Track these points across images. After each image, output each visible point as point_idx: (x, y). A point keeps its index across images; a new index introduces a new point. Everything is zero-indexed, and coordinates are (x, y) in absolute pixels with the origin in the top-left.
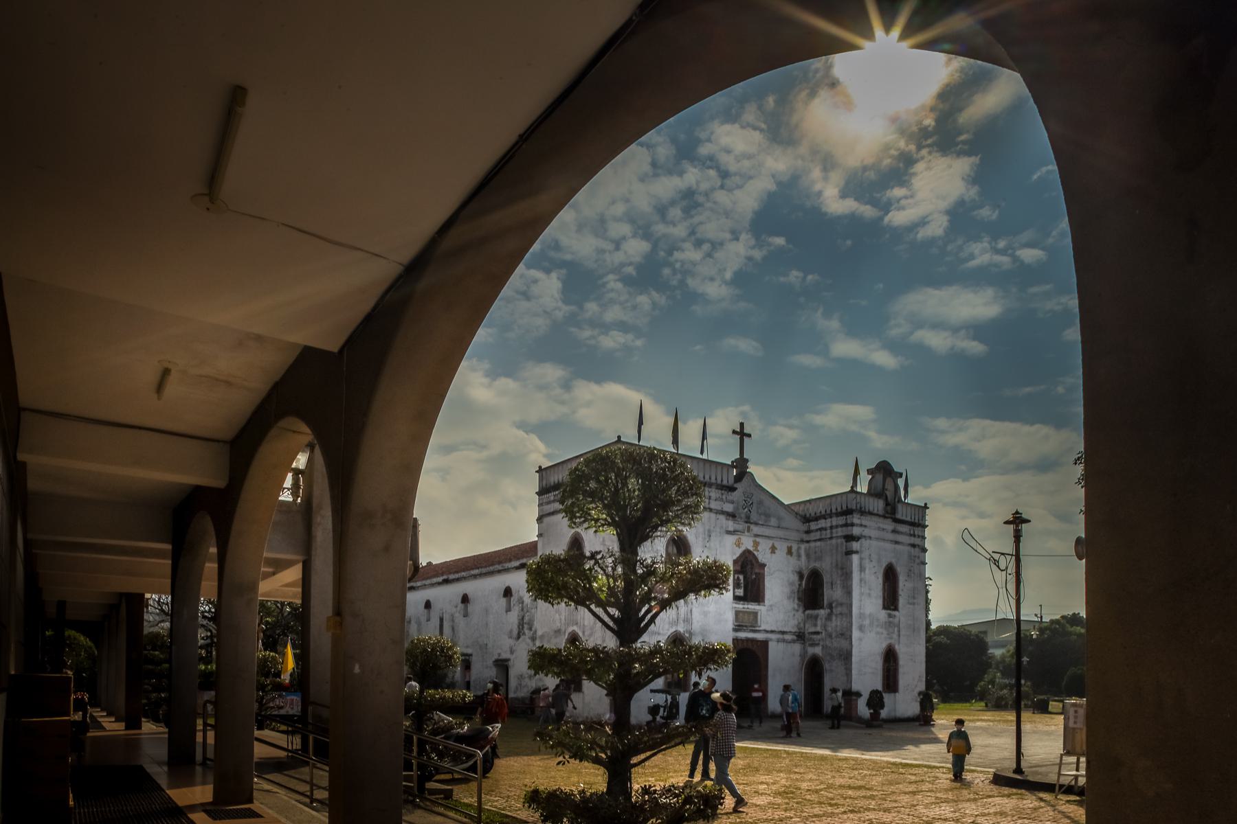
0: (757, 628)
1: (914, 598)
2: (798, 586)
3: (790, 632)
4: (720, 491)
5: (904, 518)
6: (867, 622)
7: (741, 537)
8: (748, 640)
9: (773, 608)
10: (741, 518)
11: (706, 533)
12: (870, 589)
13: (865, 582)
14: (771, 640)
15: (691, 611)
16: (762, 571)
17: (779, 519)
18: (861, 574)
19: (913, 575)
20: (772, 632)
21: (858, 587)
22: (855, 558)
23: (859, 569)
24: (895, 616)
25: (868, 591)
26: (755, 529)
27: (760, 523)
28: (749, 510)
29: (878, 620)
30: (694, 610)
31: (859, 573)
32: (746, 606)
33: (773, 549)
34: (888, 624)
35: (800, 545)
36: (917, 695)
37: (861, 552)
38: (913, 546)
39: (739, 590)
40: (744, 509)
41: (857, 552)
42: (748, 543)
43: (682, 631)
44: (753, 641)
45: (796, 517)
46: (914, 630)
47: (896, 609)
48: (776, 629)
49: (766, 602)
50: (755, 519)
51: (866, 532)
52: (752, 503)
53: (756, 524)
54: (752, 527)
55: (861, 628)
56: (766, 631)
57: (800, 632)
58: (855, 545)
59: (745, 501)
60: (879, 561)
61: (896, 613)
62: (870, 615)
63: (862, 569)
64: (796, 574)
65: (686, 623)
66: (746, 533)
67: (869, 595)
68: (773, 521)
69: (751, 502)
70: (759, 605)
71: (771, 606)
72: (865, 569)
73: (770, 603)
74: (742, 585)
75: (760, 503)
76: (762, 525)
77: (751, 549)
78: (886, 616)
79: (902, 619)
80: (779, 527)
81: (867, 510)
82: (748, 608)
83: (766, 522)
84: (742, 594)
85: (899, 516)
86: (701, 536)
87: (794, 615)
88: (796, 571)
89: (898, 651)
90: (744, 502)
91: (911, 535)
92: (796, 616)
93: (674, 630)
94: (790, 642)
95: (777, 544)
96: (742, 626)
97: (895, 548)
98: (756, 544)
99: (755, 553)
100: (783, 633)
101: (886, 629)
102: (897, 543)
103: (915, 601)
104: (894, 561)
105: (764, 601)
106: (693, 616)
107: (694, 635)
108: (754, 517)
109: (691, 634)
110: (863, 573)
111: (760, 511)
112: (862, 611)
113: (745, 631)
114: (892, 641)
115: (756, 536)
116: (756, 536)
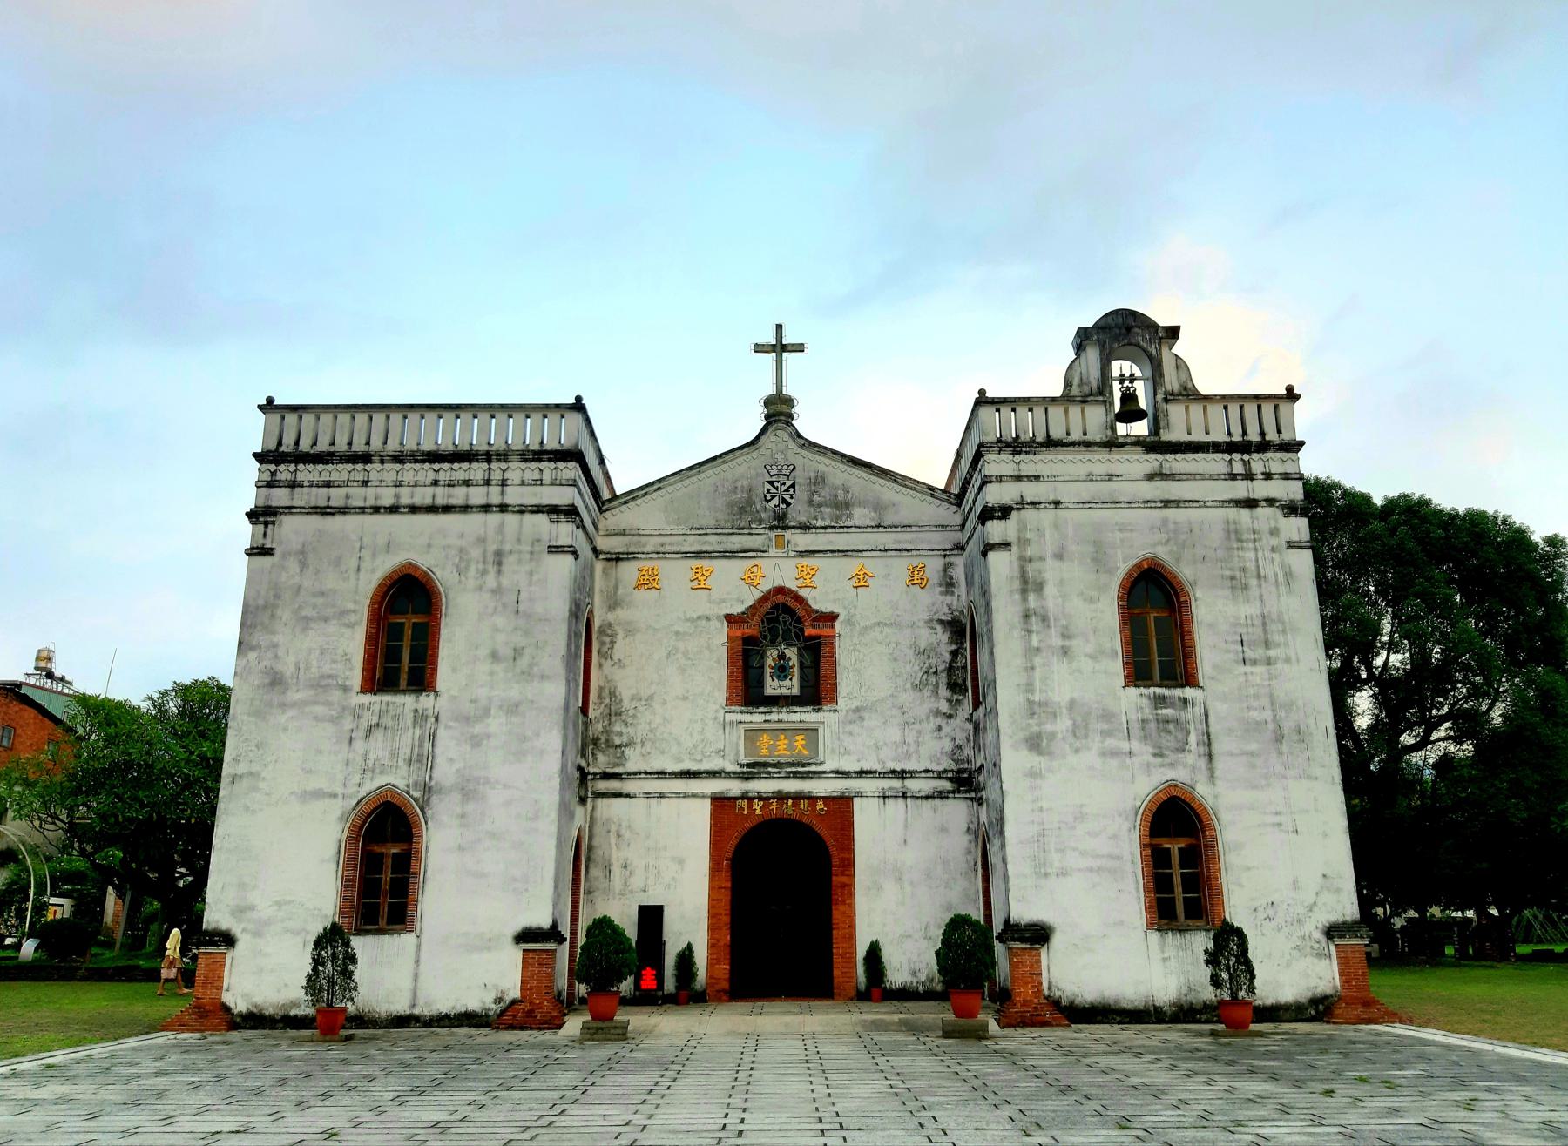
0: (813, 768)
1: (1267, 644)
2: (948, 658)
3: (927, 771)
4: (533, 465)
5: (1198, 436)
6: (1063, 725)
8: (781, 797)
9: (864, 714)
10: (761, 521)
11: (490, 559)
12: (1065, 636)
13: (1044, 619)
14: (859, 794)
15: (433, 738)
16: (825, 631)
17: (879, 507)
18: (1025, 599)
19: (1254, 582)
20: (861, 774)
21: (1017, 633)
22: (1000, 565)
23: (1017, 584)
24: (1185, 701)
25: (1057, 642)
26: (802, 540)
27: (820, 523)
28: (784, 501)
29: (1108, 716)
30: (441, 733)
31: (1017, 596)
32: (774, 717)
34: (1153, 725)
35: (952, 559)
36: (1318, 935)
37: (1024, 543)
38: (1251, 503)
39: (787, 683)
40: (768, 501)
41: (1006, 545)
42: (779, 572)
43: (401, 784)
44: (798, 797)
45: (933, 496)
46: (1279, 738)
47: (1190, 680)
48: (878, 768)
49: (842, 703)
50: (803, 519)
51: (1030, 491)
52: (793, 486)
53: (805, 528)
54: (788, 534)
55: (1035, 743)
56: (843, 774)
57: (960, 771)
58: (996, 530)
59: (771, 483)
60: (1099, 560)
61: (1189, 692)
62: (1072, 705)
63: (1028, 584)
64: (939, 628)
65: (415, 766)
66: (773, 552)
67: (1065, 651)
68: (860, 515)
69: (789, 483)
70: (819, 710)
71: (857, 710)
72: (1039, 587)
73: (856, 703)
74: (796, 670)
75: (819, 481)
76: (824, 528)
77: (792, 585)
78: (1145, 702)
79: (1218, 709)
80: (878, 526)
81: (1040, 438)
82: (780, 721)
83: (838, 518)
84: (796, 691)
85: (1175, 432)
86: (473, 568)
87: (939, 728)
88: (941, 622)
89: (1209, 803)
90: (769, 487)
91: (1233, 477)
92: (946, 729)
93: (381, 781)
94: (927, 797)
96: (765, 765)
97: (1165, 521)
99: (803, 593)
100: (901, 775)
101: (1145, 738)
102: (1167, 503)
103: (1272, 653)
104: (1164, 554)
105: (833, 700)
106: (438, 750)
107: (439, 792)
108: (798, 513)
109: (427, 789)
110: (1032, 597)
111: (816, 498)
112: (1037, 697)
113: (770, 776)
114: (1180, 775)
115: (803, 554)
116: (803, 554)
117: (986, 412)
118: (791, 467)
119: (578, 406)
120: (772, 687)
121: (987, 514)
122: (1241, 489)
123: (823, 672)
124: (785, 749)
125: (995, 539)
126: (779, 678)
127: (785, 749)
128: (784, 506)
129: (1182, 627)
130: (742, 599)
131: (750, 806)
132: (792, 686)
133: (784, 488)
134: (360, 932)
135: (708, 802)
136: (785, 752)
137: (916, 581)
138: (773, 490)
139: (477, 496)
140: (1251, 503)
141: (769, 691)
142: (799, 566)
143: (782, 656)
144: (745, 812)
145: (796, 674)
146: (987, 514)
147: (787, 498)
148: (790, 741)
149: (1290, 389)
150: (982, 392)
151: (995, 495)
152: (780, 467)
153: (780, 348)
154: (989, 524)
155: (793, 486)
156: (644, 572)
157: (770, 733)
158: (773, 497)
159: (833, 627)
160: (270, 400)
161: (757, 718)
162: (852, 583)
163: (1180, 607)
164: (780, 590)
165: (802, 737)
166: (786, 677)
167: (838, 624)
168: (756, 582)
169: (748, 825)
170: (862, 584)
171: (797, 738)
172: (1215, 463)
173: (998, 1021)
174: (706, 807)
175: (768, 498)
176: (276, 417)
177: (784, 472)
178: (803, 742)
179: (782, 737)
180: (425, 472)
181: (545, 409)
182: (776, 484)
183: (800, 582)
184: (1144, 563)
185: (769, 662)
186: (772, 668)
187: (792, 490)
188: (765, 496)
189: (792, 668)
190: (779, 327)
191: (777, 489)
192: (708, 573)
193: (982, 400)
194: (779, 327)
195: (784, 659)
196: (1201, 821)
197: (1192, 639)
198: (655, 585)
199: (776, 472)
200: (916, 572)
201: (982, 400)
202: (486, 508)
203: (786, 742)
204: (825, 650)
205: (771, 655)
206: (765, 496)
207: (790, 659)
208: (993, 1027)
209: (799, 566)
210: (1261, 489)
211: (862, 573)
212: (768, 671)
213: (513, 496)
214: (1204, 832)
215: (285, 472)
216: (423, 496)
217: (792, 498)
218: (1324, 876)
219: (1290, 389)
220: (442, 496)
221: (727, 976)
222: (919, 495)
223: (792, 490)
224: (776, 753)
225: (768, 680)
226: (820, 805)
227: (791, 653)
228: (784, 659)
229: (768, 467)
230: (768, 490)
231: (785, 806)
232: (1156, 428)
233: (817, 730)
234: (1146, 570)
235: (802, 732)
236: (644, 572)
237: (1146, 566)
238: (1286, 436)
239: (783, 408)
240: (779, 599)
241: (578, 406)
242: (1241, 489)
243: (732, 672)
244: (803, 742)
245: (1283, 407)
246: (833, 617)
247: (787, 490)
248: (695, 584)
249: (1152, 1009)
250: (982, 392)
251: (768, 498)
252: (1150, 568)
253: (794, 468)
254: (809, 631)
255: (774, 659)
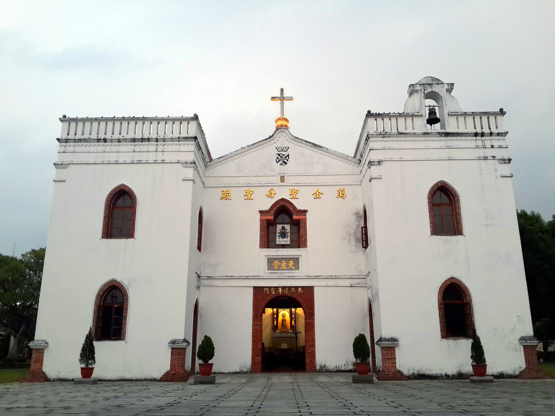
5: (462, 130)
7: (272, 188)
33: (317, 196)
38: (486, 158)
39: (285, 239)
40: (277, 162)
52: (288, 156)
58: (375, 171)
59: (279, 155)
74: (289, 234)
77: (288, 198)
84: (289, 243)
90: (278, 156)
91: (478, 147)
95: (321, 190)
98: (294, 193)
99: (293, 201)
117: (371, 121)
118: (287, 148)
119: (196, 118)
120: (279, 241)
121: (371, 163)
122: (481, 153)
123: (301, 234)
124: (285, 267)
125: (375, 175)
126: (282, 237)
127: (285, 267)
128: (284, 164)
129: (456, 211)
130: (267, 205)
131: (270, 290)
132: (287, 241)
133: (284, 157)
134: (99, 339)
135: (252, 289)
136: (284, 268)
137: (341, 196)
138: (279, 158)
139: (151, 157)
140: (486, 158)
141: (278, 243)
142: (291, 190)
143: (283, 228)
144: (268, 293)
145: (289, 236)
146: (371, 163)
147: (286, 161)
148: (287, 264)
149: (501, 110)
150: (369, 112)
151: (374, 156)
152: (282, 148)
153: (282, 98)
154: (372, 167)
155: (288, 156)
156: (224, 192)
157: (278, 260)
158: (279, 161)
159: (305, 215)
160: (65, 116)
161: (273, 252)
162: (314, 196)
163: (455, 202)
164: (283, 200)
165: (292, 261)
166: (285, 237)
167: (307, 214)
168: (272, 196)
169: (269, 298)
170: (317, 197)
171: (290, 262)
172: (470, 142)
173: (377, 378)
174: (251, 291)
175: (277, 161)
176: (67, 124)
177: (284, 150)
178: (293, 264)
179: (284, 261)
180: (129, 147)
181: (181, 120)
182: (281, 155)
183: (291, 197)
184: (439, 183)
185: (278, 230)
186: (279, 233)
187: (287, 157)
188: (276, 160)
189: (287, 233)
190: (282, 90)
191: (281, 157)
192: (252, 193)
193: (369, 114)
194: (282, 90)
195: (284, 230)
196: (465, 294)
197: (460, 216)
198: (229, 198)
199: (281, 150)
200: (341, 192)
201: (369, 114)
202: (155, 162)
203: (285, 263)
204: (302, 225)
205: (279, 227)
206: (276, 160)
207: (287, 229)
208: (375, 379)
209: (291, 190)
210: (490, 153)
211: (317, 192)
212: (278, 234)
213: (168, 157)
214: (466, 298)
215: (70, 147)
216: (128, 157)
217: (287, 161)
218: (518, 316)
219: (501, 110)
220: (137, 157)
221: (260, 362)
222: (342, 159)
223: (287, 157)
224: (281, 268)
225: (277, 238)
226: (300, 289)
227: (288, 227)
228: (284, 230)
229: (277, 148)
230: (277, 158)
231: (285, 290)
232: (443, 127)
233: (299, 258)
234: (440, 186)
235: (292, 259)
236: (224, 192)
237: (440, 185)
238: (500, 131)
239: (284, 123)
240: (282, 203)
241: (196, 118)
242: (481, 153)
243: (262, 234)
244: (293, 264)
245: (499, 118)
246: (305, 211)
247: (286, 157)
248: (246, 198)
249: (444, 375)
250: (369, 112)
251: (277, 161)
252: (442, 186)
253: (289, 148)
254: (295, 217)
255: (280, 230)
